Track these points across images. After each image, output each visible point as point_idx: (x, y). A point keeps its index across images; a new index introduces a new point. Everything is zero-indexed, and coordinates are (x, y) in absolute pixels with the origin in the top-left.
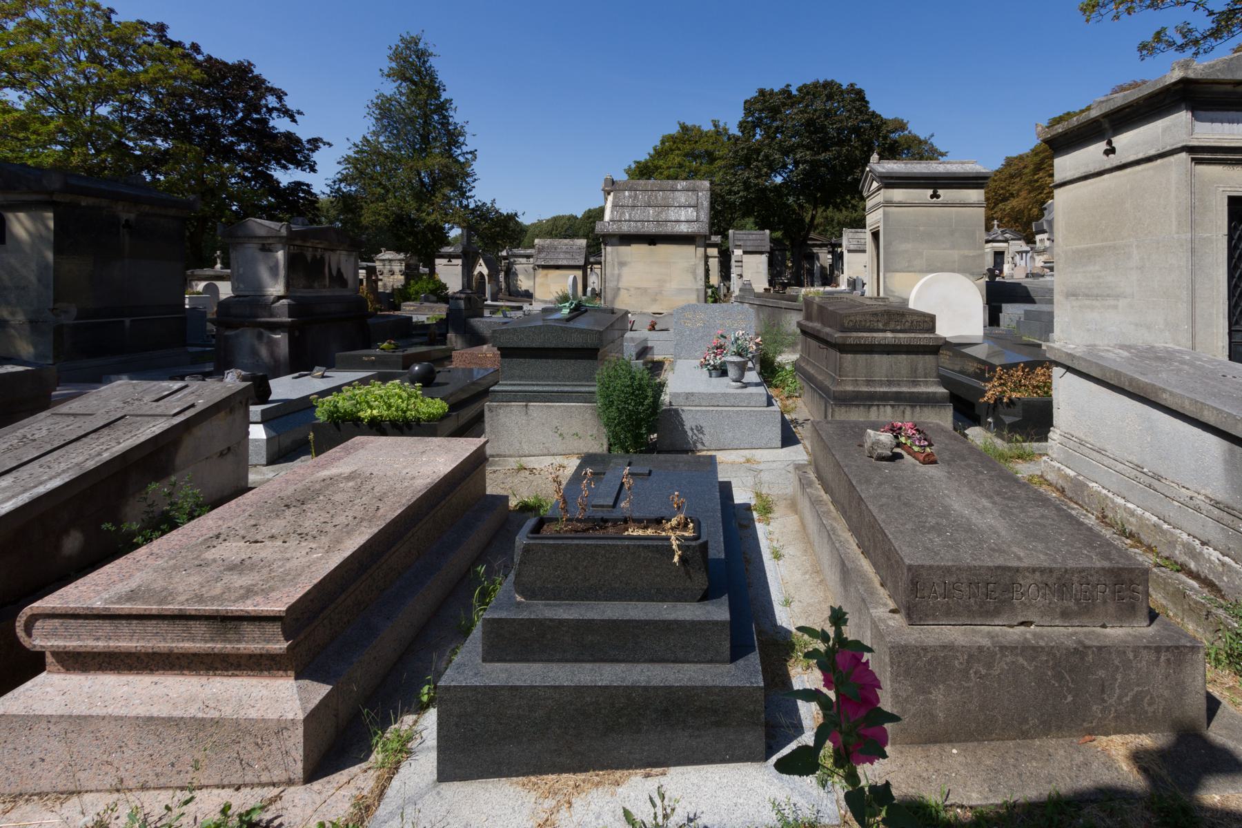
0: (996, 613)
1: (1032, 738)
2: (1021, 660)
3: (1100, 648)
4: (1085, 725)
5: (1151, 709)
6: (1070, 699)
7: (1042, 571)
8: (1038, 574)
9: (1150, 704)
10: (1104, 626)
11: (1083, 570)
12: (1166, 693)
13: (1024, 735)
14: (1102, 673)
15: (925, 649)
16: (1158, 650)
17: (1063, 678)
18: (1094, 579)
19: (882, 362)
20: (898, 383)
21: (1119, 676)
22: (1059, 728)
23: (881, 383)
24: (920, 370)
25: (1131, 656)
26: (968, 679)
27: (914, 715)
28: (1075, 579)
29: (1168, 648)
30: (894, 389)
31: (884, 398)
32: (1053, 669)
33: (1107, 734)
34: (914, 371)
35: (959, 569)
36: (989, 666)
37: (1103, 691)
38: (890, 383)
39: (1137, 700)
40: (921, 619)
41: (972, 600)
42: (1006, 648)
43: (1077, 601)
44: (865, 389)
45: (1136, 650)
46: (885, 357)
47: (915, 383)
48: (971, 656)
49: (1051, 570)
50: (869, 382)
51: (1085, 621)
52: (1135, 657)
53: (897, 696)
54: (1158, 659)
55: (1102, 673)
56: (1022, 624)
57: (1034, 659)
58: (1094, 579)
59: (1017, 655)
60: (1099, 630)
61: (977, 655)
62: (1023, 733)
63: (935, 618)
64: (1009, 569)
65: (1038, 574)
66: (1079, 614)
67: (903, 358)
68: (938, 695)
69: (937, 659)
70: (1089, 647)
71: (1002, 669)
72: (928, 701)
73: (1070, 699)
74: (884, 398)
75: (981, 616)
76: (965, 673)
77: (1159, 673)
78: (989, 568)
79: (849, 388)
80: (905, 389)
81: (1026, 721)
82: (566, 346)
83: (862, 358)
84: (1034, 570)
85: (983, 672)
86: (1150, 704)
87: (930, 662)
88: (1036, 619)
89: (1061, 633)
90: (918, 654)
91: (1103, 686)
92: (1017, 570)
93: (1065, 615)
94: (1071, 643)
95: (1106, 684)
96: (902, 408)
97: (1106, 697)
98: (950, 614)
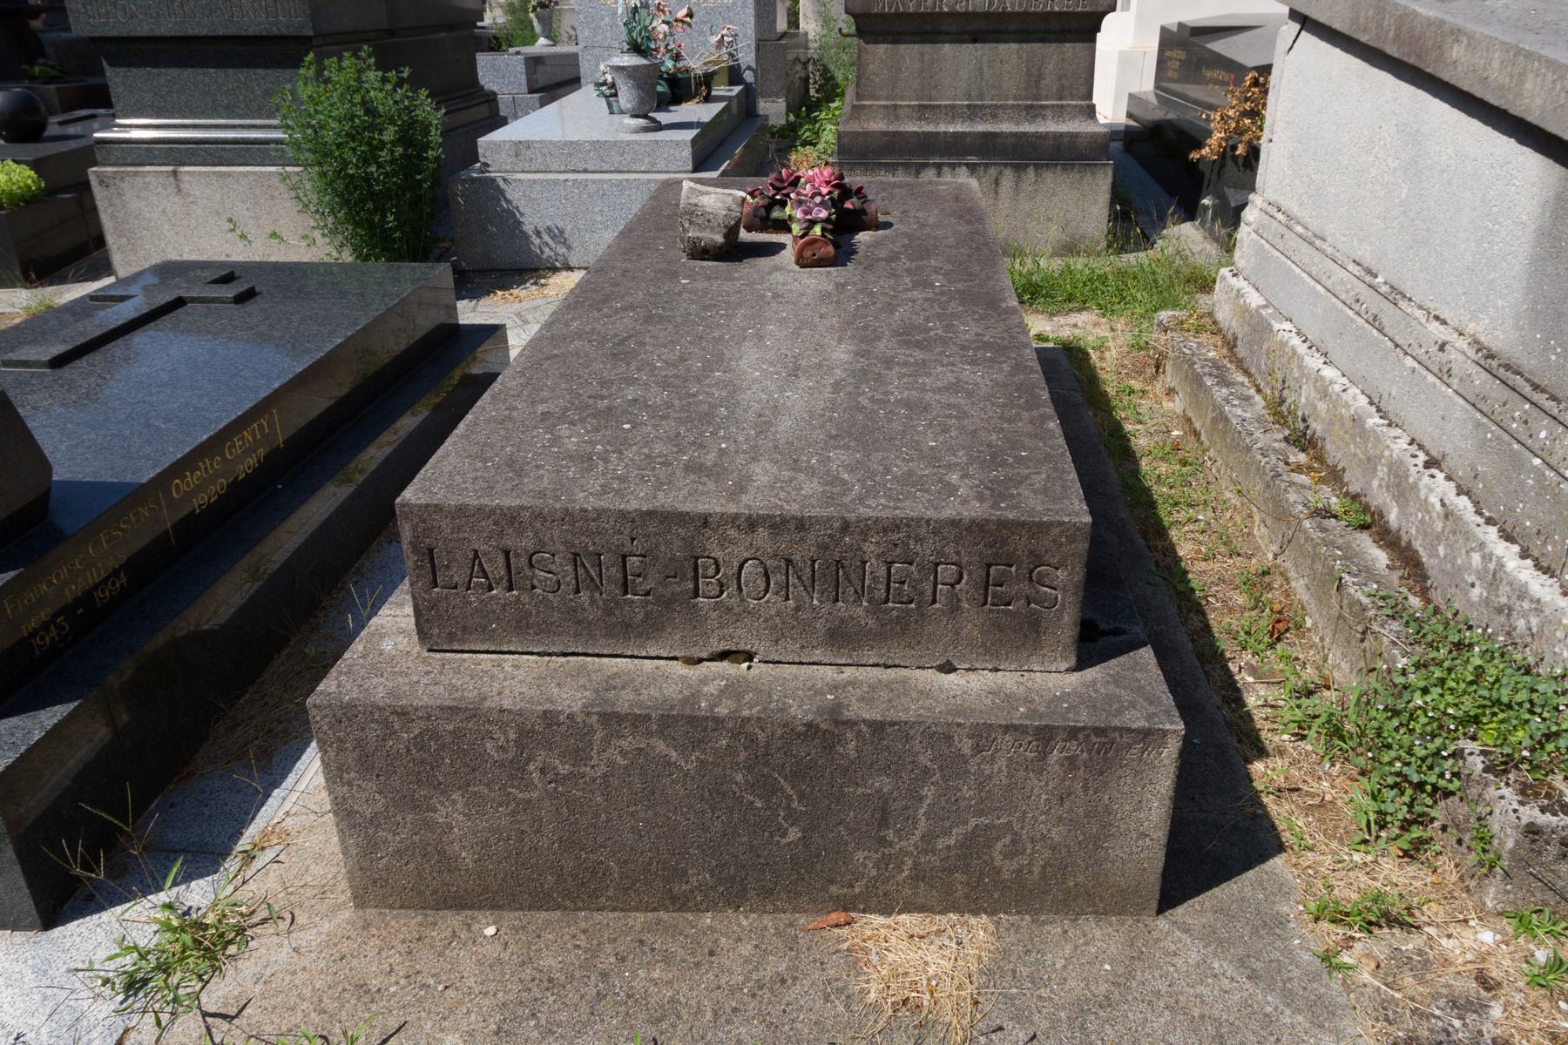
0: (651, 627)
1: (699, 909)
2: (661, 746)
3: (878, 727)
4: (834, 889)
5: (1008, 868)
6: (794, 834)
7: (778, 525)
8: (762, 533)
9: (1009, 855)
10: (948, 668)
11: (896, 526)
12: (1056, 834)
13: (680, 903)
14: (882, 783)
15: (402, 713)
16: (1045, 735)
17: (776, 789)
18: (925, 551)
19: (959, 63)
20: (994, 113)
21: (929, 792)
22: (768, 893)
23: (953, 113)
24: (1049, 82)
25: (967, 747)
26: (528, 786)
27: (399, 853)
28: (869, 548)
29: (1073, 733)
30: (981, 128)
31: (954, 150)
32: (750, 768)
33: (887, 911)
34: (1034, 81)
35: (538, 515)
36: (579, 755)
37: (884, 822)
38: (973, 112)
39: (975, 844)
40: (451, 637)
41: (584, 596)
42: (621, 718)
43: (877, 606)
44: (912, 127)
45: (983, 735)
46: (969, 48)
47: (1033, 112)
48: (525, 734)
49: (802, 525)
50: (923, 111)
51: (897, 655)
52: (978, 749)
53: (350, 813)
54: (1043, 755)
55: (882, 783)
56: (723, 656)
57: (695, 744)
58: (925, 551)
59: (649, 734)
60: (931, 678)
61: (541, 729)
62: (674, 899)
63: (490, 636)
64: (683, 518)
65: (762, 533)
66: (878, 637)
67: (1008, 50)
68: (452, 813)
69: (435, 736)
70: (850, 724)
71: (611, 764)
72: (429, 825)
73: (794, 834)
74: (954, 150)
75: (609, 635)
76: (517, 770)
77: (1041, 789)
78: (623, 515)
79: (877, 125)
80: (1006, 127)
81: (682, 875)
82: (232, 30)
83: (910, 53)
84: (752, 523)
85: (564, 769)
86: (1009, 855)
87: (419, 742)
88: (762, 648)
89: (796, 681)
90: (386, 724)
91: (884, 811)
92: (705, 521)
93: (841, 638)
94: (801, 711)
95: (894, 806)
96: (993, 171)
97: (890, 835)
98: (526, 628)
